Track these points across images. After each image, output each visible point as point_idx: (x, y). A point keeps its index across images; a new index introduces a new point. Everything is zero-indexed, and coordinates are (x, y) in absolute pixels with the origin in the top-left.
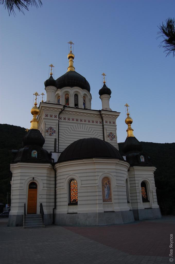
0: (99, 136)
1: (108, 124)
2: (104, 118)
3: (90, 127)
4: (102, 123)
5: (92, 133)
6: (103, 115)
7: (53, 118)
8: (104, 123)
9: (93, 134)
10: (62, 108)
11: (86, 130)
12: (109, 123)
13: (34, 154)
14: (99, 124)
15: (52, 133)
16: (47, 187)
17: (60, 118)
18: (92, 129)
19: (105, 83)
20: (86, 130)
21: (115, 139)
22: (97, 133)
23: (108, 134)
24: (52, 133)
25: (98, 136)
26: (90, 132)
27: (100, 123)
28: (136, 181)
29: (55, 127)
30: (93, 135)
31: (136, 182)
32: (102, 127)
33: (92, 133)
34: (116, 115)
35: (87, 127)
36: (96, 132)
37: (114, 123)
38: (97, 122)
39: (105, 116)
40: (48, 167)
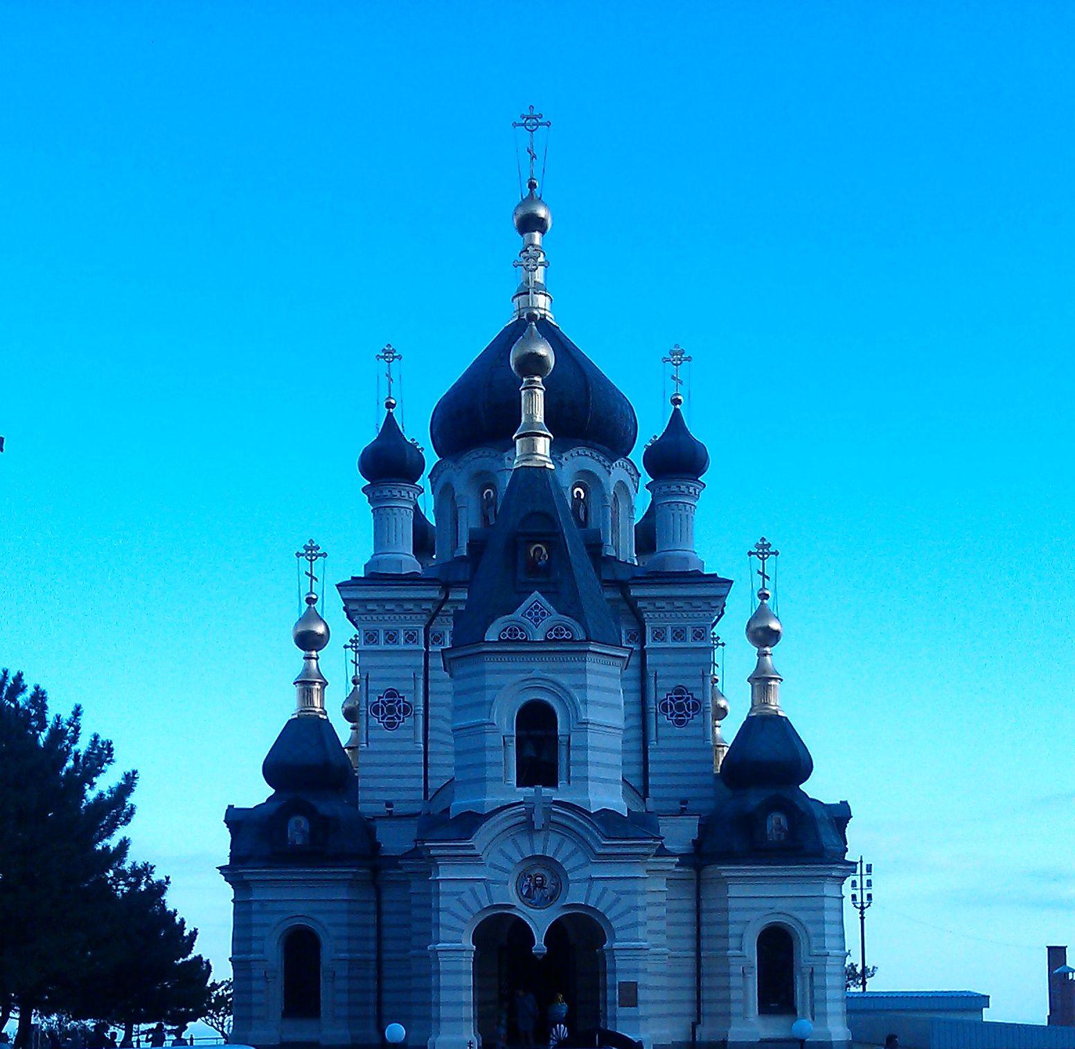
1: (670, 644)
2: (645, 615)
6: (640, 604)
7: (402, 645)
8: (649, 644)
10: (435, 594)
13: (297, 829)
15: (397, 716)
16: (349, 951)
17: (436, 639)
19: (679, 402)
21: (698, 718)
24: (397, 716)
28: (731, 926)
29: (410, 686)
31: (733, 929)
34: (713, 590)
37: (700, 634)
39: (651, 608)
40: (350, 876)
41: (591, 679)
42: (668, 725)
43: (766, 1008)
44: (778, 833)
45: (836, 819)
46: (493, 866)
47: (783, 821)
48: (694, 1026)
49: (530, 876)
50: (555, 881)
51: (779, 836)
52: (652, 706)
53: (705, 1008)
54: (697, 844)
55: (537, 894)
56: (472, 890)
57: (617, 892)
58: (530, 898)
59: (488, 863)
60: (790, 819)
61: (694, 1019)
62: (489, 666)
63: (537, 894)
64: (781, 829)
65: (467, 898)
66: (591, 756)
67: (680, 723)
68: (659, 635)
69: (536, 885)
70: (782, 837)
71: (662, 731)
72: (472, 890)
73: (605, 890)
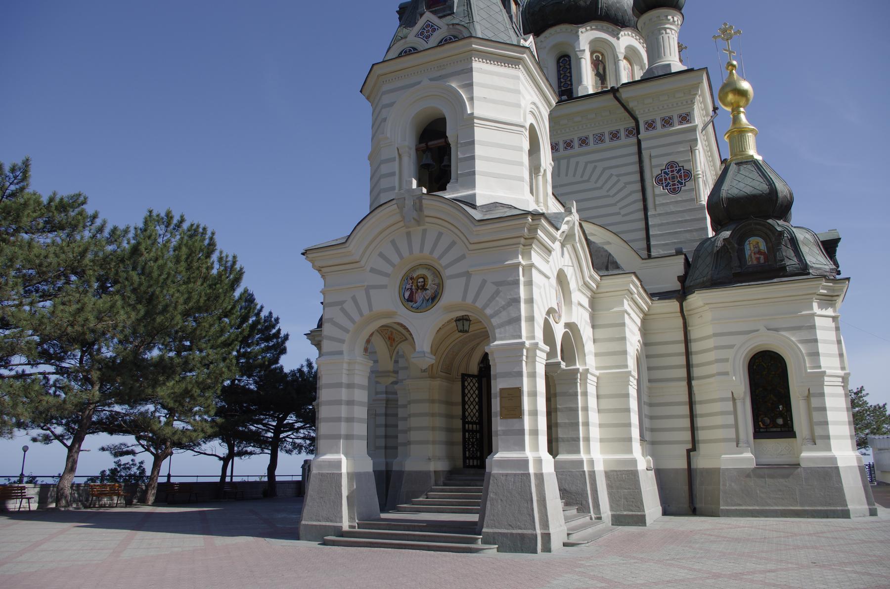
0: (624, 187)
2: (637, 113)
3: (586, 164)
4: (635, 131)
5: (596, 182)
9: (599, 184)
11: (574, 176)
12: (681, 123)
14: (624, 140)
18: (595, 167)
20: (574, 176)
22: (618, 176)
23: (657, 171)
25: (620, 185)
26: (588, 181)
27: (629, 133)
30: (601, 188)
32: (635, 149)
33: (596, 182)
35: (577, 163)
36: (612, 175)
38: (615, 136)
41: (477, 77)
42: (665, 194)
43: (760, 432)
44: (758, 256)
45: (823, 243)
46: (373, 270)
47: (763, 246)
48: (689, 451)
49: (412, 279)
50: (437, 281)
51: (758, 259)
52: (650, 182)
53: (701, 435)
54: (682, 279)
55: (419, 296)
56: (354, 299)
57: (494, 283)
58: (412, 301)
59: (368, 269)
60: (766, 239)
61: (690, 446)
62: (385, 88)
63: (419, 296)
64: (760, 252)
65: (349, 306)
66: (479, 150)
67: (674, 191)
68: (650, 125)
69: (418, 288)
70: (762, 261)
71: (659, 200)
72: (354, 299)
73: (484, 282)
